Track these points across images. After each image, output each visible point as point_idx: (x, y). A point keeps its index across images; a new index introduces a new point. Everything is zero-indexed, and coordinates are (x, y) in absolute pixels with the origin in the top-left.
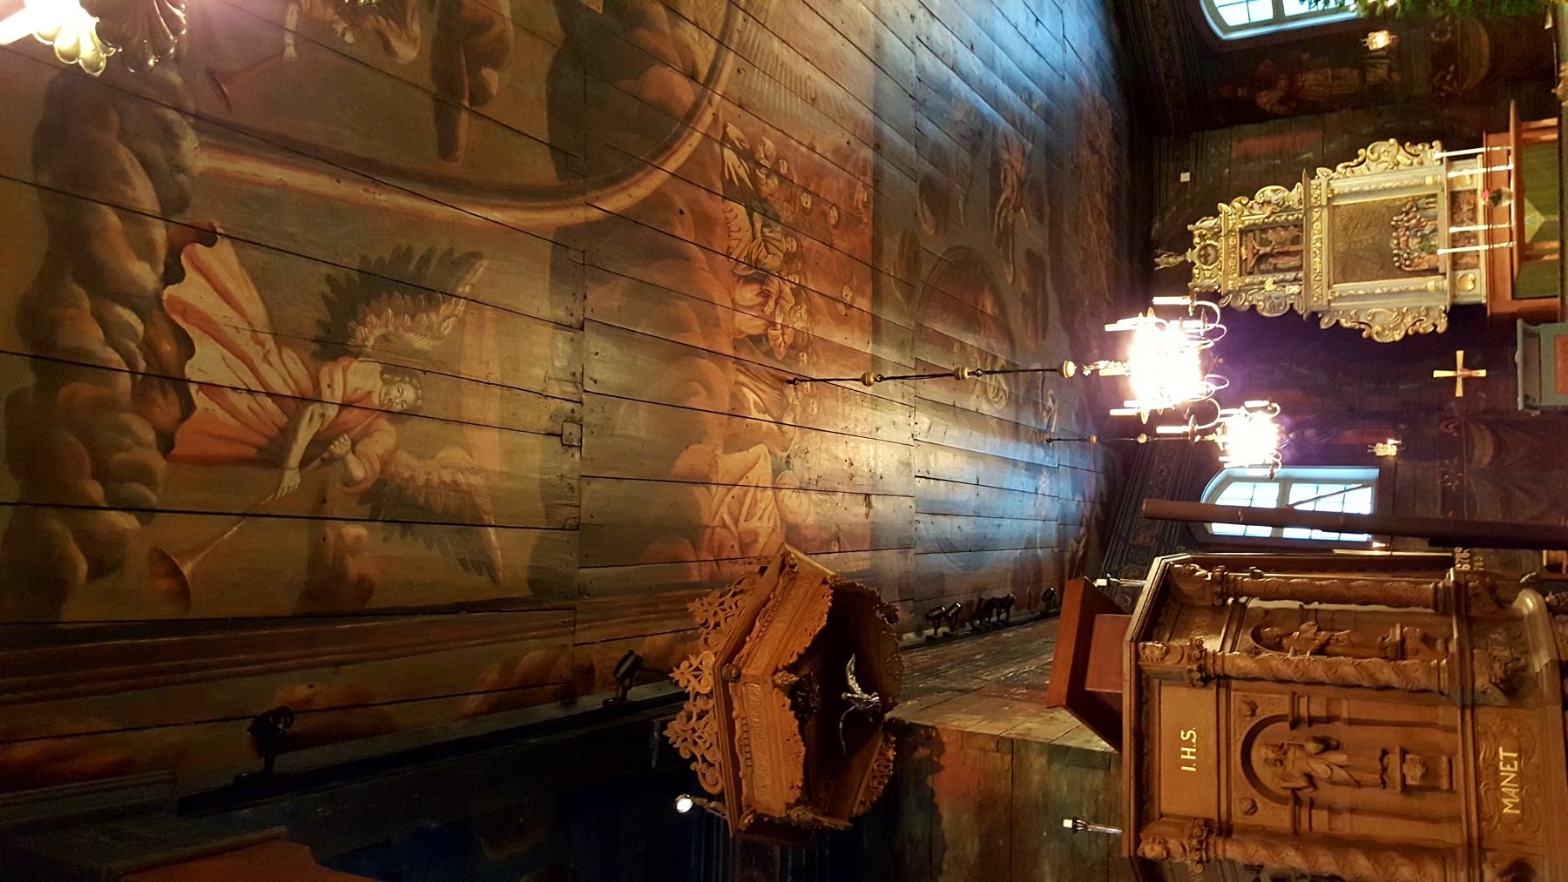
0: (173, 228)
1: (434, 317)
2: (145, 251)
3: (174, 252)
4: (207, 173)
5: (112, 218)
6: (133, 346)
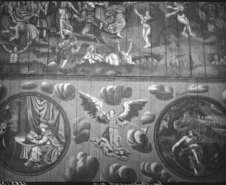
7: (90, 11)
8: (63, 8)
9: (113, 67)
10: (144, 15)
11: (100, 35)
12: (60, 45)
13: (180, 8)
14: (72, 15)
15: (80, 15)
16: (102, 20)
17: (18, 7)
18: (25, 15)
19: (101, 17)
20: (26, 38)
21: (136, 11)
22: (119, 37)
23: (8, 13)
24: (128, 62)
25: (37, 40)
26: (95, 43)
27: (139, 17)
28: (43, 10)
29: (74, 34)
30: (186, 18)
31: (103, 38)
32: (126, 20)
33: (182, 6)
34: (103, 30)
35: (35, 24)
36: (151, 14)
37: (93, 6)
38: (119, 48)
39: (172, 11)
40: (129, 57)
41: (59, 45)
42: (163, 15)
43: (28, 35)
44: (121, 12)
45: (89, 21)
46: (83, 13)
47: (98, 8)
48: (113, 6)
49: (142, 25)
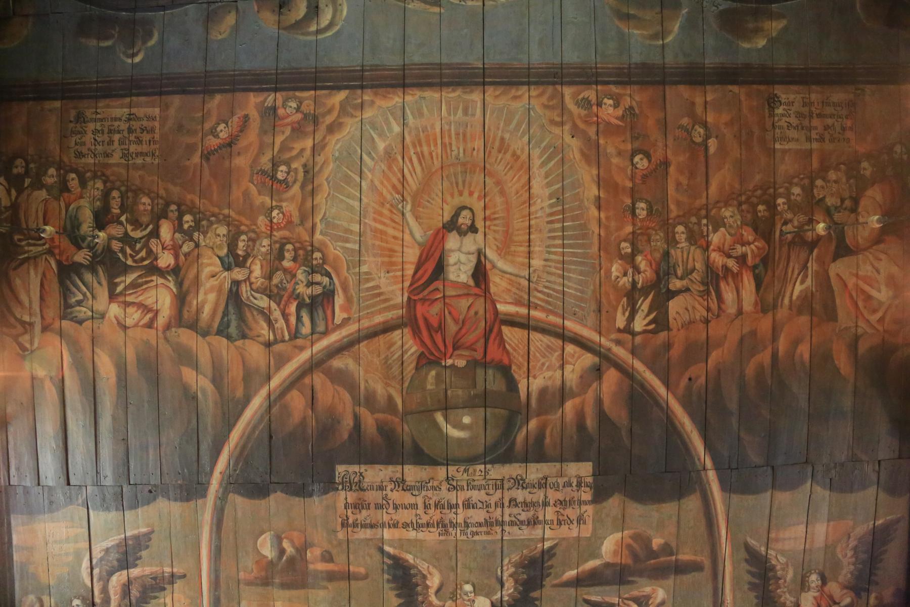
1: (778, 567)
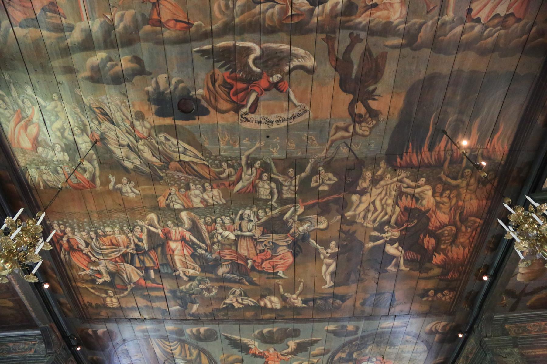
0: (467, 21)
2: (472, 28)
3: (474, 20)
4: (454, 13)
5: (464, 36)
6: (494, 30)
7: (228, 245)
8: (176, 241)
9: (272, 310)
10: (327, 247)
11: (248, 275)
12: (182, 288)
13: (394, 235)
14: (195, 250)
15: (209, 250)
16: (251, 256)
17: (94, 240)
18: (110, 251)
19: (248, 251)
20: (123, 280)
21: (313, 242)
22: (280, 278)
23: (78, 247)
24: (296, 305)
25: (143, 282)
26: (242, 286)
27: (316, 249)
28: (140, 244)
29: (204, 274)
30: (400, 248)
31: (254, 279)
32: (295, 255)
33: (397, 231)
34: (253, 268)
35: (132, 263)
36: (338, 245)
37: (232, 236)
38: (281, 290)
39: (377, 239)
40: (297, 299)
41: (181, 288)
42: (362, 245)
43: (125, 276)
44: (285, 244)
45: (228, 258)
46: (215, 247)
47: (243, 240)
48: (270, 236)
49: (322, 261)
